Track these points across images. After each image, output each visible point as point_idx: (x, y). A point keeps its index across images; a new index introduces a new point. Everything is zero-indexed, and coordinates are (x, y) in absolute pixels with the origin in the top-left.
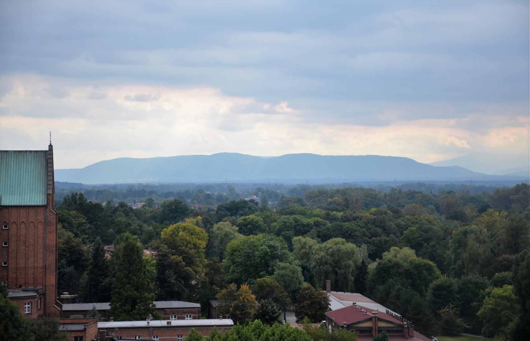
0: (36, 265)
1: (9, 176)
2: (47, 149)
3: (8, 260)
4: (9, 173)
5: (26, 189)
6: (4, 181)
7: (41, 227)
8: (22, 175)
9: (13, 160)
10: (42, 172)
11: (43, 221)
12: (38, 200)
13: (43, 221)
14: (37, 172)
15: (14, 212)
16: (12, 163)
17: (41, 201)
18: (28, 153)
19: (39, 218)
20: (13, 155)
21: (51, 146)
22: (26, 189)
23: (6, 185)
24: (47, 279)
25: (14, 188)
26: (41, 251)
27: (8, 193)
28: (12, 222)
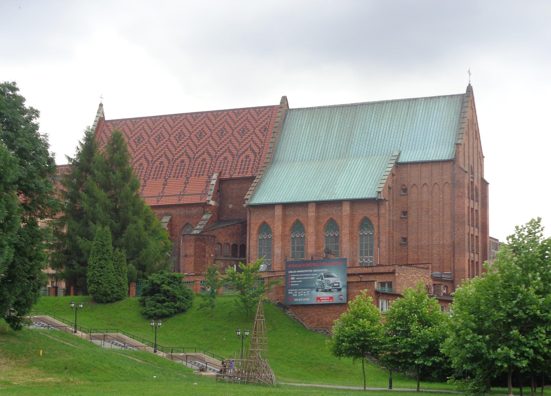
0: (441, 243)
1: (414, 128)
2: (464, 91)
3: (407, 234)
4: (415, 125)
5: (432, 142)
6: (407, 134)
7: (447, 189)
8: (430, 125)
9: (421, 108)
10: (455, 120)
11: (450, 182)
12: (445, 154)
13: (450, 182)
14: (449, 120)
15: (414, 171)
16: (421, 111)
17: (448, 155)
18: (441, 98)
19: (445, 177)
20: (423, 103)
21: (470, 89)
22: (432, 142)
23: (409, 138)
24: (456, 261)
25: (417, 142)
26: (448, 222)
27: (410, 148)
28: (412, 184)
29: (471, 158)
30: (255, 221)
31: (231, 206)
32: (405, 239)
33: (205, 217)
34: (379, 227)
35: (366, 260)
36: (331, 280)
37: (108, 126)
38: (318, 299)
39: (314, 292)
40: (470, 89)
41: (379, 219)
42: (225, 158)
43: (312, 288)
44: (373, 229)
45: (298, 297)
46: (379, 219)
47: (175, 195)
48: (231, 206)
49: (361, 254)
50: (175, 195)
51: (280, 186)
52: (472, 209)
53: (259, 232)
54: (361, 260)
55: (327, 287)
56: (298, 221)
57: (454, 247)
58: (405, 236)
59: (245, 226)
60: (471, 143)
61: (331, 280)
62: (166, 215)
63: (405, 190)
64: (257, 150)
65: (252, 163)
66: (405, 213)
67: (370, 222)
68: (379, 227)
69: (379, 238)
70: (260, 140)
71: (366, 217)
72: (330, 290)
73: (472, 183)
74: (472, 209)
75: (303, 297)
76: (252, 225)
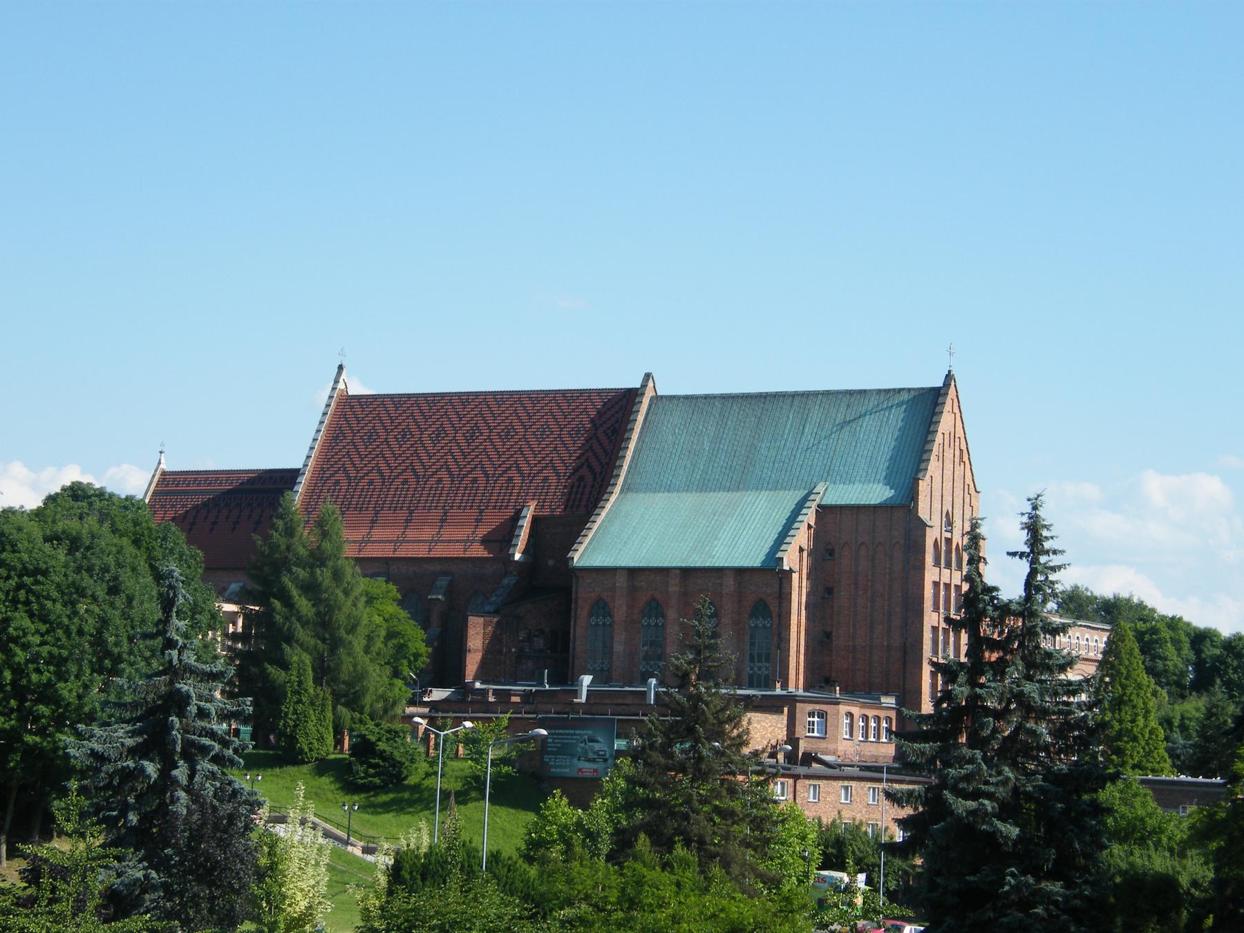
13: (902, 542)
26: (897, 610)
29: (948, 498)
30: (584, 594)
31: (551, 563)
32: (828, 635)
33: (505, 581)
34: (780, 616)
35: (760, 669)
36: (597, 746)
37: (352, 407)
38: (580, 770)
39: (575, 760)
40: (949, 377)
41: (780, 603)
42: (546, 479)
43: (573, 755)
44: (771, 617)
45: (556, 767)
46: (780, 603)
47: (457, 541)
48: (551, 563)
49: (752, 659)
50: (457, 541)
51: (634, 532)
52: (947, 586)
53: (591, 615)
54: (752, 669)
55: (591, 755)
56: (653, 599)
57: (905, 652)
58: (829, 629)
59: (569, 601)
60: (948, 473)
61: (597, 746)
62: (444, 573)
63: (831, 553)
64: (598, 469)
65: (588, 490)
66: (830, 591)
67: (766, 606)
68: (780, 616)
69: (779, 634)
70: (605, 451)
71: (761, 600)
72: (594, 761)
73: (949, 541)
74: (947, 586)
75: (561, 767)
76: (580, 602)
